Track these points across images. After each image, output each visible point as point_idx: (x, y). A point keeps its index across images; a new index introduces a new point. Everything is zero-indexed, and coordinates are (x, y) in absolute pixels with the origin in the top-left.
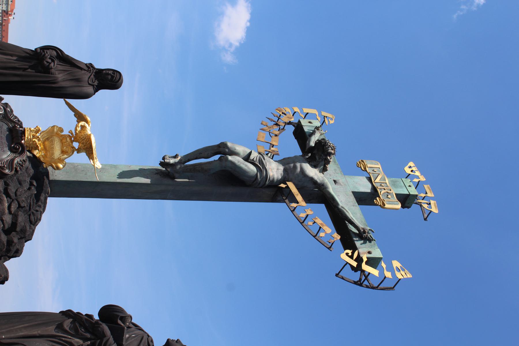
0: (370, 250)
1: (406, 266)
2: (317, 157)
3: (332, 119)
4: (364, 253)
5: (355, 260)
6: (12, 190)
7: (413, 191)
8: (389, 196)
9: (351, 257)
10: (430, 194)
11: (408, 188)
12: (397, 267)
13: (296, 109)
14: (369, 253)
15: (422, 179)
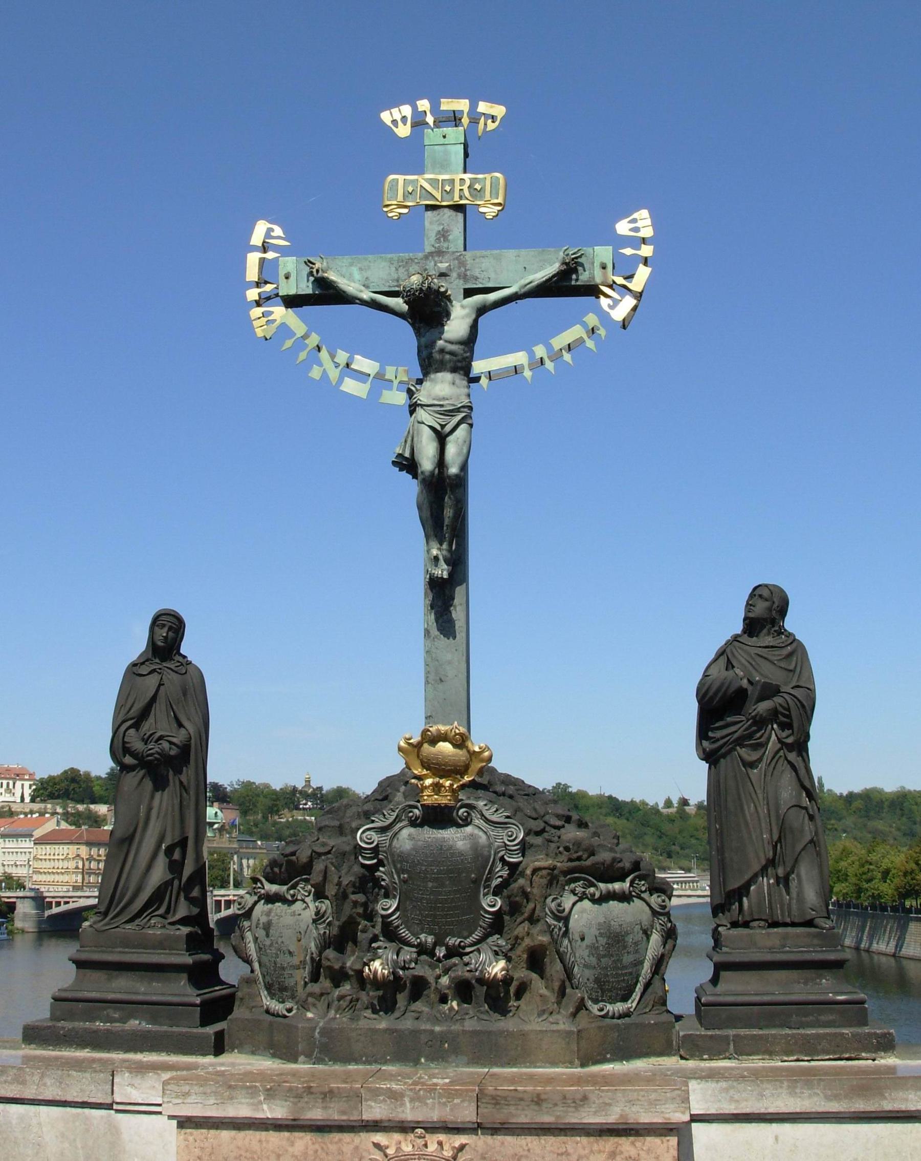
0: (597, 265)
1: (625, 213)
2: (437, 309)
3: (270, 230)
4: (605, 275)
5: (623, 297)
6: (538, 825)
7: (455, 134)
8: (478, 186)
9: (616, 303)
10: (462, 105)
11: (446, 141)
12: (631, 230)
13: (253, 294)
14: (604, 267)
15: (424, 105)
